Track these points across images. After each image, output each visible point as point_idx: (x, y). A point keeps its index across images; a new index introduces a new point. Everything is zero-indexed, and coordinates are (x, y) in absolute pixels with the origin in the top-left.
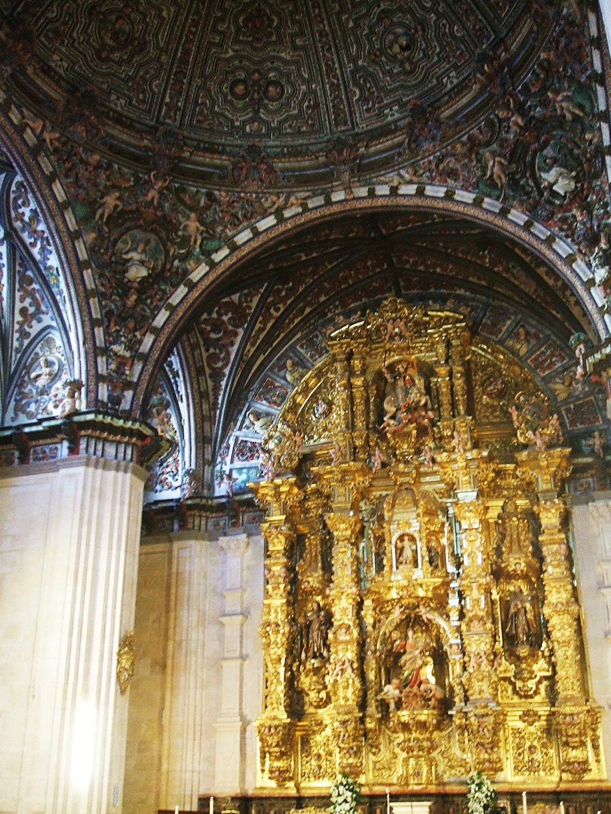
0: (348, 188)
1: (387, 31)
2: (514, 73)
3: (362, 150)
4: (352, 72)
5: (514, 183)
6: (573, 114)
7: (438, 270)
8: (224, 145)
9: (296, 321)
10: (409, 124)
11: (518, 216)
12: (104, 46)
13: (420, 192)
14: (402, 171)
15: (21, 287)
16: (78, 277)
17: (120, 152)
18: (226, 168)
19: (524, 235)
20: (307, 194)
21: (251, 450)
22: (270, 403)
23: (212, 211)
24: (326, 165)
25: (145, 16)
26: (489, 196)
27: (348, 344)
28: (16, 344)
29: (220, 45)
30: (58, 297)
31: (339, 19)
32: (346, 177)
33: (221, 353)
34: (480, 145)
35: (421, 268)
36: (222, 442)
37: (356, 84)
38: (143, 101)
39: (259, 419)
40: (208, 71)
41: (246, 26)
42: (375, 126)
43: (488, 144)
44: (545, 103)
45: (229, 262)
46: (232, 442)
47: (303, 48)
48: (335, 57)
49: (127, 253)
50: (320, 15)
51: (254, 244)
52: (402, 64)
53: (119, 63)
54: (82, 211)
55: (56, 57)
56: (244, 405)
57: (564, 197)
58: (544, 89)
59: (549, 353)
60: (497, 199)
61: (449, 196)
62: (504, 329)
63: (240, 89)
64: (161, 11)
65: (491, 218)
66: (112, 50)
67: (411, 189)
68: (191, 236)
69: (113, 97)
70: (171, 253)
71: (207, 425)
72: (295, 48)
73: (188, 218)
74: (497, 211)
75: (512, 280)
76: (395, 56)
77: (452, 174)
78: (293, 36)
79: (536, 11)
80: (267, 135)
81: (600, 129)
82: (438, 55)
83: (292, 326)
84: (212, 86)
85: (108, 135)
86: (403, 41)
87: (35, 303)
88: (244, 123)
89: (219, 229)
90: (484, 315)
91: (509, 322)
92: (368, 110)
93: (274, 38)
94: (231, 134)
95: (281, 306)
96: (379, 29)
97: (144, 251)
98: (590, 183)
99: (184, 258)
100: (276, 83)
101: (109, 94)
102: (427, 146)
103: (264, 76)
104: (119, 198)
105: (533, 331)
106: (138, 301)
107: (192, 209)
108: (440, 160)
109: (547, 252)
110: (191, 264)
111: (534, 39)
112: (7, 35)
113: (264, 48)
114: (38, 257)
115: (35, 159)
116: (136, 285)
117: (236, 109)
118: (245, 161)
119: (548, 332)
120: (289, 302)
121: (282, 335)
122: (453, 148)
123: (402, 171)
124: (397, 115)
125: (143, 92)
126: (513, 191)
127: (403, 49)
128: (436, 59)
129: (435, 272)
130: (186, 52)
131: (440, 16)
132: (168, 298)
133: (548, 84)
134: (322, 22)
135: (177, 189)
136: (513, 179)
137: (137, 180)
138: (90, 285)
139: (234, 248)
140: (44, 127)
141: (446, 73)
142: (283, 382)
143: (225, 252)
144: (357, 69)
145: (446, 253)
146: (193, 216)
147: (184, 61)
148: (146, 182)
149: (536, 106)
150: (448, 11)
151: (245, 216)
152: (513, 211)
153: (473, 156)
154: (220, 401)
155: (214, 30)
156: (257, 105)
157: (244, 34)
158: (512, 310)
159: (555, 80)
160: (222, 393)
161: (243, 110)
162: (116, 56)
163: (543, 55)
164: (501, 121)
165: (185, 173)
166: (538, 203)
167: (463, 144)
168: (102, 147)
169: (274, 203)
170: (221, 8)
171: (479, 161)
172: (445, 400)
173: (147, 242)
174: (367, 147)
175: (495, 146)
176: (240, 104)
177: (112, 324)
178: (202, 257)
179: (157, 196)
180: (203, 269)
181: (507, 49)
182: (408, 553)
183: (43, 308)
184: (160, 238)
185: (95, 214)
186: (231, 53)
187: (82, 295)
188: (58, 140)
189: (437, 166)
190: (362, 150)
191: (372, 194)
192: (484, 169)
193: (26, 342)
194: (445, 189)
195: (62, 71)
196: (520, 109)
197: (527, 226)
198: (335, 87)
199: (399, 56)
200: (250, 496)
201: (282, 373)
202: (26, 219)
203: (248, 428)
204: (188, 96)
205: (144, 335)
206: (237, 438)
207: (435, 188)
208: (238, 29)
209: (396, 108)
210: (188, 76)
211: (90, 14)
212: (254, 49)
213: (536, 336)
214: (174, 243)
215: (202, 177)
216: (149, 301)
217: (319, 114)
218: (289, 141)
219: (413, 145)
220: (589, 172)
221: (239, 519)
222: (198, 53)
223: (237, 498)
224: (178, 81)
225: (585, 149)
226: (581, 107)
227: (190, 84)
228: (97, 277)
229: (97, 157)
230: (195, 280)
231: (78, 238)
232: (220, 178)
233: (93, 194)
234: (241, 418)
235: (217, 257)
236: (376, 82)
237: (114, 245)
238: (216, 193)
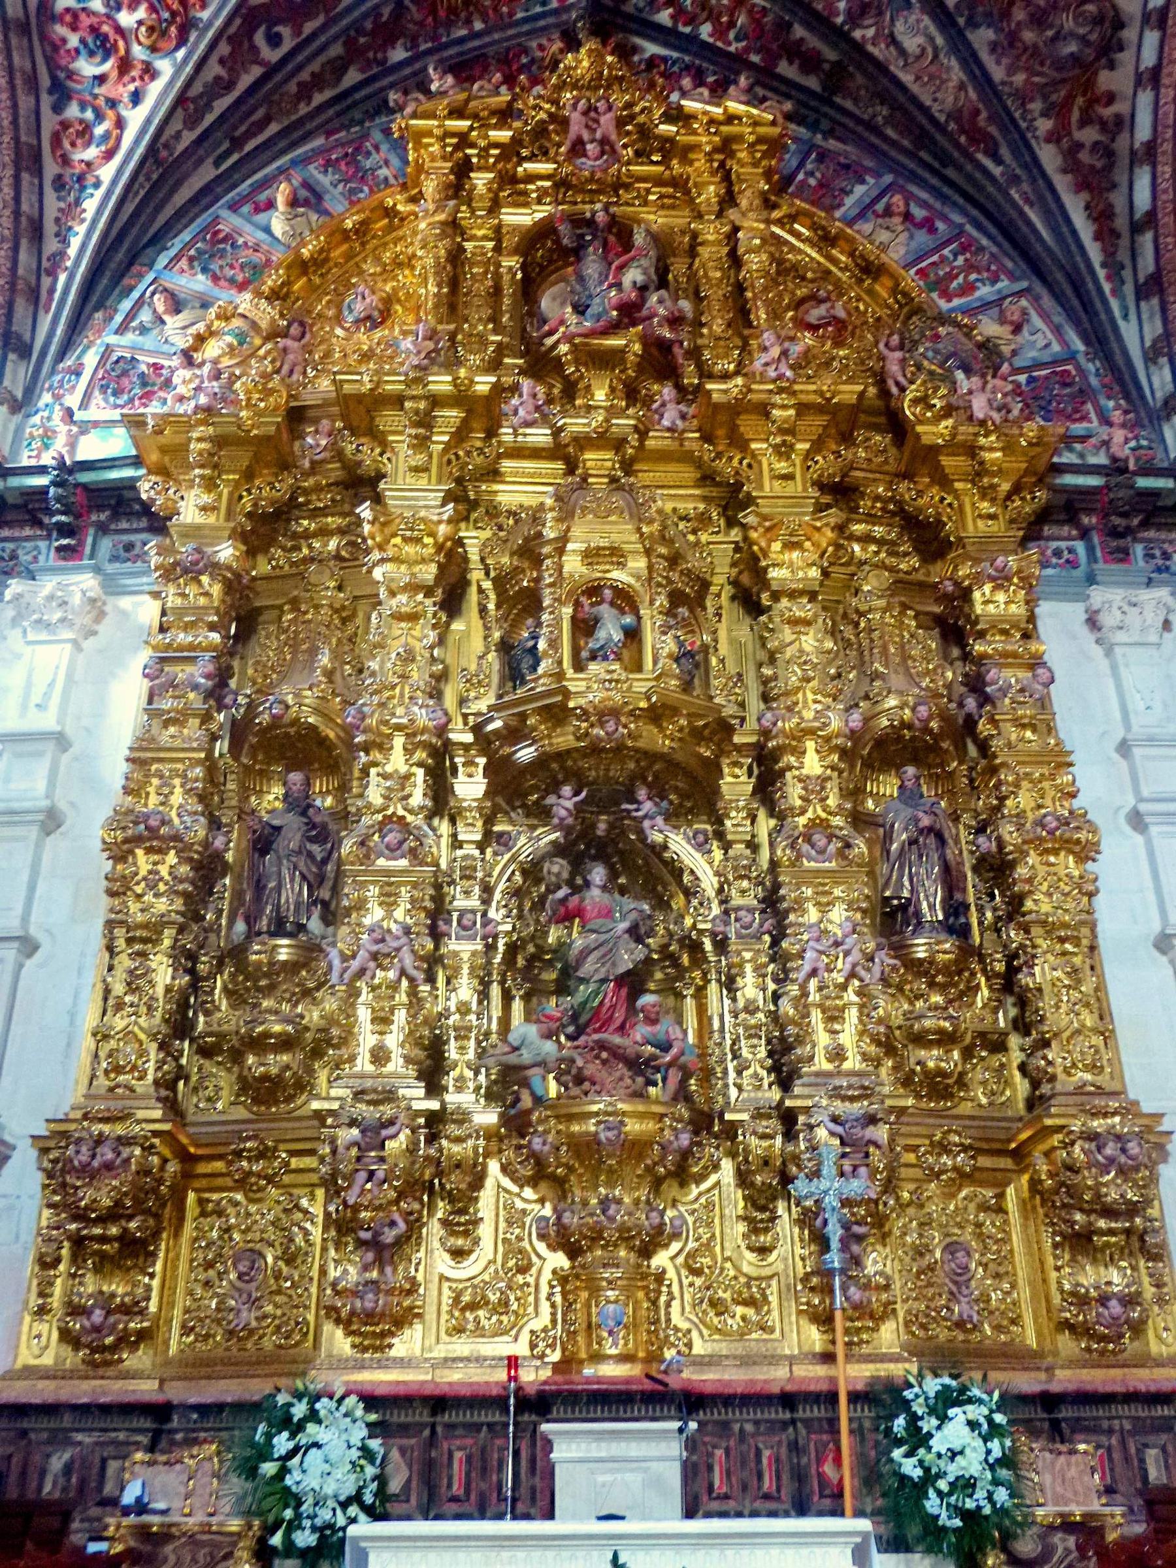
9: (318, 99)
21: (144, 380)
22: (215, 279)
27: (464, 140)
33: (100, 117)
36: (62, 355)
39: (178, 311)
46: (91, 359)
56: (141, 276)
59: (960, 261)
62: (849, 201)
71: (21, 308)
83: (303, 109)
90: (801, 165)
91: (859, 190)
95: (285, 31)
105: (919, 213)
119: (957, 218)
120: (309, 27)
121: (273, 128)
129: (694, 38)
142: (261, 235)
154: (72, 251)
158: (869, 163)
160: (81, 229)
172: (716, 292)
182: (610, 630)
200: (128, 473)
201: (261, 218)
203: (143, 330)
206: (109, 349)
213: (928, 225)
221: (81, 543)
223: (85, 477)
234: (126, 305)
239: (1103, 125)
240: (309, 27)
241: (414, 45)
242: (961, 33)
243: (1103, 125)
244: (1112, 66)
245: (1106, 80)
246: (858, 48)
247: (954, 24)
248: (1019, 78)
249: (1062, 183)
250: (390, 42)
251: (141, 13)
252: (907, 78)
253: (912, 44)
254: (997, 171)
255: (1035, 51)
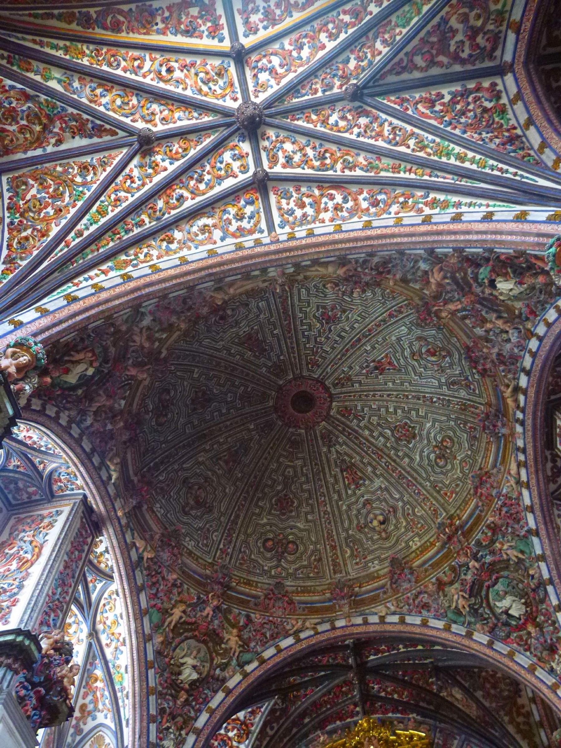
0: (348, 617)
1: (369, 513)
2: (467, 534)
3: (357, 589)
4: (346, 539)
5: (474, 611)
6: (517, 557)
7: (396, 696)
8: (257, 582)
9: (285, 740)
10: (391, 571)
11: (482, 638)
12: (188, 504)
13: (402, 621)
14: (388, 604)
15: (87, 683)
16: (144, 674)
17: (190, 577)
18: (259, 597)
19: (488, 651)
20: (317, 621)
23: (248, 629)
24: (330, 600)
25: (216, 490)
26: (455, 622)
28: (69, 740)
29: (259, 515)
30: (119, 694)
31: (337, 504)
32: (346, 609)
34: (445, 584)
35: (383, 694)
37: (347, 546)
38: (207, 546)
40: (249, 531)
41: (276, 504)
42: (362, 574)
43: (451, 583)
44: (493, 553)
45: (258, 673)
47: (313, 521)
48: (333, 528)
49: (182, 658)
50: (324, 501)
51: (277, 659)
52: (380, 533)
53: (195, 517)
54: (156, 617)
55: (158, 505)
57: (519, 619)
58: (493, 542)
60: (463, 625)
61: (424, 624)
63: (270, 543)
64: (225, 488)
65: (458, 639)
66: (192, 508)
67: (395, 619)
68: (231, 649)
69: (187, 539)
70: (215, 662)
72: (307, 521)
73: (231, 633)
74: (464, 634)
75: (456, 703)
76: (374, 529)
77: (426, 606)
78: (306, 514)
79: (481, 494)
80: (286, 578)
81: (539, 567)
82: (405, 527)
84: (251, 540)
85: (183, 563)
86: (381, 518)
87: (95, 701)
88: (271, 568)
89: (252, 644)
91: (456, 742)
92: (357, 564)
93: (293, 514)
94: (261, 575)
96: (364, 511)
97: (195, 658)
98: (537, 607)
99: (224, 667)
100: (293, 542)
101: (186, 536)
102: (406, 585)
103: (286, 538)
104: (184, 612)
106: (187, 702)
107: (233, 626)
108: (417, 596)
109: (511, 664)
110: (226, 674)
111: (481, 511)
112: (139, 481)
113: (288, 519)
114: (109, 656)
115: (133, 571)
116: (187, 686)
117: (267, 559)
118: (274, 594)
120: (281, 722)
122: (425, 586)
123: (388, 604)
124: (378, 567)
125: (207, 538)
126: (474, 617)
127: (382, 523)
128: (403, 530)
129: (393, 698)
130: (237, 517)
131: (405, 504)
132: (209, 702)
133: (495, 538)
134: (325, 505)
135: (225, 609)
136: (473, 608)
137: (199, 598)
138: (152, 684)
139: (262, 661)
140: (145, 549)
141: (411, 539)
143: (255, 664)
144: (349, 536)
145: (404, 681)
146: (235, 631)
147: (235, 522)
148: (204, 602)
149: (486, 555)
150: (411, 499)
151: (272, 636)
152: (475, 633)
153: (441, 593)
155: (257, 505)
156: (280, 557)
157: (275, 510)
159: (500, 536)
161: (271, 559)
162: (193, 512)
163: (491, 519)
164: (460, 566)
165: (230, 598)
166: (496, 625)
167: (433, 584)
168: (178, 571)
169: (293, 626)
170: (262, 491)
171: (445, 596)
173: (199, 652)
174: (360, 587)
175: (457, 585)
176: (269, 555)
177: (164, 720)
178: (237, 668)
179: (211, 613)
180: (238, 678)
181: (460, 519)
183: (100, 706)
184: (208, 648)
185: (164, 622)
186: (265, 520)
187: (145, 690)
188: (152, 559)
189: (414, 600)
190: (357, 589)
191: (366, 623)
192: (451, 601)
193: (78, 738)
194: (420, 618)
195: (159, 515)
196: (475, 557)
197: (490, 645)
198: (333, 548)
199: (377, 528)
202: (108, 623)
204: (235, 545)
205: (187, 734)
207: (413, 618)
208: (272, 505)
209: (376, 562)
210: (237, 532)
211: (184, 482)
212: (281, 520)
214: (218, 654)
215: (242, 603)
216: (194, 703)
217: (322, 565)
218: (301, 583)
219: (394, 586)
220: (535, 599)
222: (244, 518)
224: (230, 535)
225: (529, 584)
226: (522, 552)
227: (237, 539)
228: (158, 676)
229: (175, 576)
230: (231, 687)
231: (149, 640)
232: (256, 605)
233: (166, 605)
235: (249, 668)
236: (362, 545)
237: (174, 650)
238: (252, 615)
239: (523, 715)
240: (281, 722)
241: (311, 716)
242: (472, 694)
243: (523, 715)
244: (520, 696)
245: (520, 701)
246: (443, 698)
247: (469, 691)
248: (494, 705)
249: (518, 737)
250: (304, 718)
251: (235, 732)
252: (460, 706)
253: (459, 696)
254: (497, 734)
255: (495, 696)
